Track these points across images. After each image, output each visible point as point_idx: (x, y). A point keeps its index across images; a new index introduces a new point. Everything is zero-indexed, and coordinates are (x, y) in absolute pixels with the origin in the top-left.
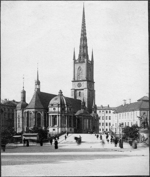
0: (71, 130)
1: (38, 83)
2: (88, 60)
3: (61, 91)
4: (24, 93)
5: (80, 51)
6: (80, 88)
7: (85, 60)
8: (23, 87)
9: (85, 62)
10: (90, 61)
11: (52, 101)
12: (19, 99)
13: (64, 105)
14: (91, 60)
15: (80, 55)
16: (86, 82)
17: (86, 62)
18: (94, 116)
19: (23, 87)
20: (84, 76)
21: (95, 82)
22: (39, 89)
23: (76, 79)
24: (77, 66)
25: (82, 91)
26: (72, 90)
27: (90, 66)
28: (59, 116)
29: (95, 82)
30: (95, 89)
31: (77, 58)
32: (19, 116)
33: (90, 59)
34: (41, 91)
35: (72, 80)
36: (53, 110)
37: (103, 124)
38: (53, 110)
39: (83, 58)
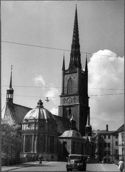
2: (80, 70)
3: (40, 101)
9: (76, 72)
10: (84, 72)
15: (70, 64)
17: (78, 73)
20: (76, 90)
21: (89, 98)
23: (66, 93)
24: (67, 77)
26: (60, 107)
28: (35, 136)
29: (89, 98)
31: (67, 67)
34: (15, 102)
36: (27, 128)
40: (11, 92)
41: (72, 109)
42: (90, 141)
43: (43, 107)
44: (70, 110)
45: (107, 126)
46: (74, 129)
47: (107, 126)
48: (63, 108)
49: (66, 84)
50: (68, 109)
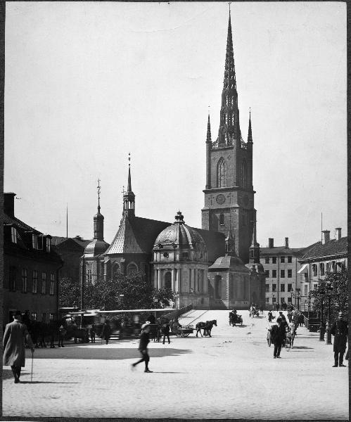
0: (202, 301)
1: (130, 197)
3: (180, 213)
4: (99, 220)
5: (222, 122)
6: (223, 206)
7: (234, 142)
8: (99, 208)
11: (161, 237)
12: (88, 234)
13: (188, 246)
14: (246, 141)
15: (221, 131)
16: (235, 194)
17: (235, 149)
18: (254, 269)
19: (99, 208)
22: (132, 212)
24: (216, 156)
25: (226, 215)
27: (245, 156)
28: (176, 270)
30: (256, 207)
32: (90, 271)
33: (245, 138)
34: (138, 214)
35: (205, 189)
37: (274, 286)
38: (163, 257)
39: (228, 137)
40: (130, 197)
41: (226, 215)
42: (257, 271)
43: (184, 223)
44: (222, 216)
45: (287, 239)
46: (233, 254)
47: (287, 239)
48: (209, 214)
49: (214, 169)
50: (218, 215)
